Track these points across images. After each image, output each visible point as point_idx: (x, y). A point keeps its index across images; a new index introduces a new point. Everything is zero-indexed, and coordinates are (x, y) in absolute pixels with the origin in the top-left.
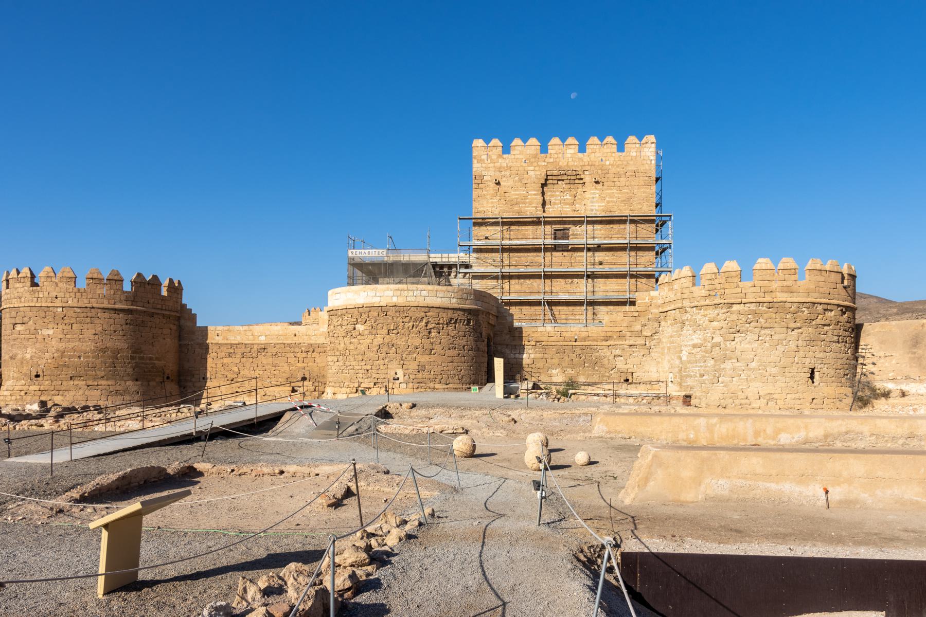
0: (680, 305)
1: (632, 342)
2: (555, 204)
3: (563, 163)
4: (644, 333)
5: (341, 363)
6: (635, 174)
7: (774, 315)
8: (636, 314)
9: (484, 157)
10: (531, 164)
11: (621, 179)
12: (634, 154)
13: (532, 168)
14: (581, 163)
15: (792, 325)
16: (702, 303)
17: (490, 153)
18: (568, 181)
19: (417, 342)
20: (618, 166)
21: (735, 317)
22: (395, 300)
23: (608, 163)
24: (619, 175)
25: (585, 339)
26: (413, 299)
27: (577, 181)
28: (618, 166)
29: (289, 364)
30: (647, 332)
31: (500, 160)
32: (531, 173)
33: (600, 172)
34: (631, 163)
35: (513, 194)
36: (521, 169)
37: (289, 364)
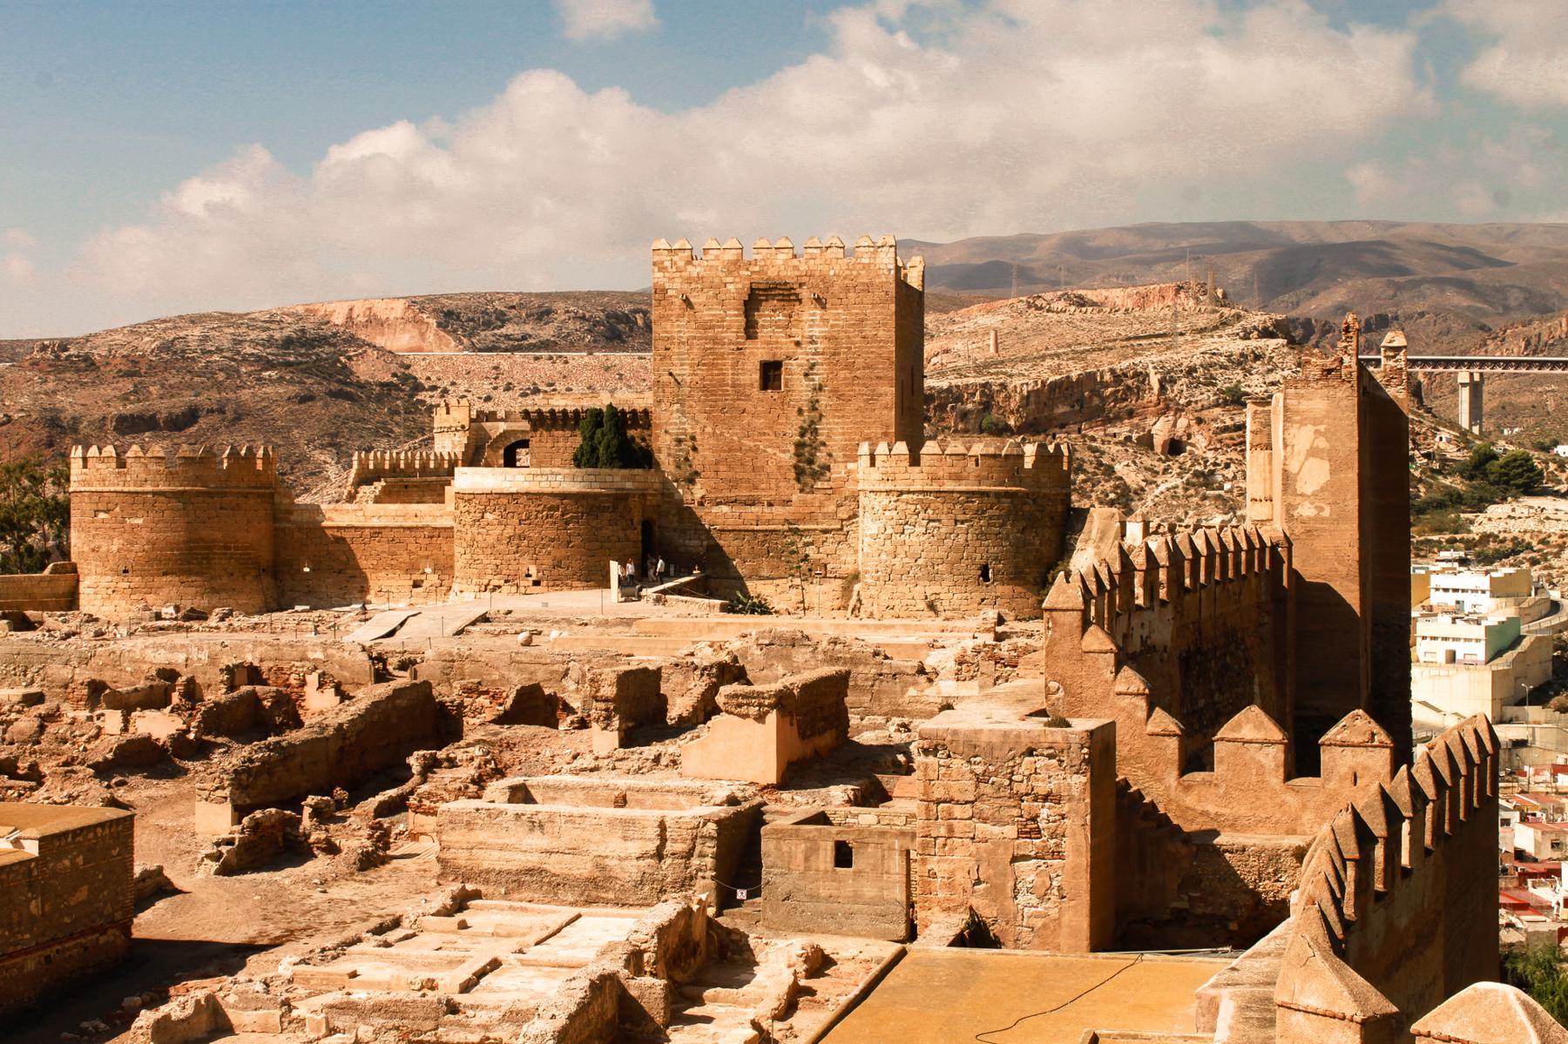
1: (825, 527)
3: (772, 273)
4: (840, 515)
5: (468, 556)
6: (868, 288)
9: (667, 264)
10: (730, 273)
13: (730, 279)
17: (676, 258)
19: (552, 533)
24: (847, 289)
25: (768, 522)
29: (410, 553)
30: (843, 514)
31: (689, 268)
35: (706, 314)
36: (716, 281)
37: (410, 553)
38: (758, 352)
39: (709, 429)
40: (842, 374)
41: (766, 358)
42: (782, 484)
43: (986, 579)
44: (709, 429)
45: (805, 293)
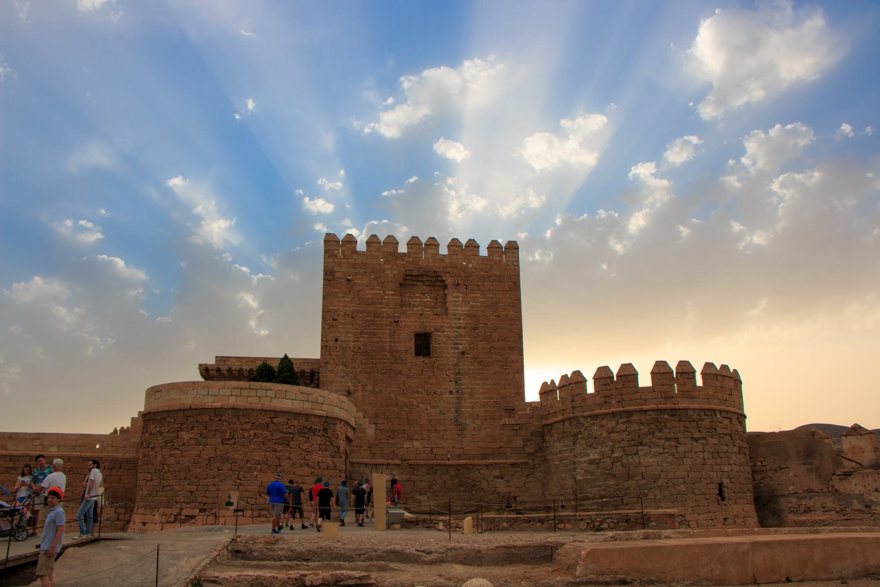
0: (571, 415)
2: (414, 306)
7: (677, 424)
8: (517, 427)
11: (485, 283)
12: (498, 258)
13: (389, 267)
14: (443, 265)
15: (696, 435)
18: (428, 283)
20: (481, 270)
21: (636, 427)
22: (232, 401)
23: (470, 266)
26: (256, 400)
27: (438, 284)
28: (481, 270)
32: (389, 272)
34: (495, 267)
38: (411, 325)
39: (369, 387)
41: (419, 330)
42: (433, 435)
43: (723, 499)
44: (369, 387)
45: (449, 281)
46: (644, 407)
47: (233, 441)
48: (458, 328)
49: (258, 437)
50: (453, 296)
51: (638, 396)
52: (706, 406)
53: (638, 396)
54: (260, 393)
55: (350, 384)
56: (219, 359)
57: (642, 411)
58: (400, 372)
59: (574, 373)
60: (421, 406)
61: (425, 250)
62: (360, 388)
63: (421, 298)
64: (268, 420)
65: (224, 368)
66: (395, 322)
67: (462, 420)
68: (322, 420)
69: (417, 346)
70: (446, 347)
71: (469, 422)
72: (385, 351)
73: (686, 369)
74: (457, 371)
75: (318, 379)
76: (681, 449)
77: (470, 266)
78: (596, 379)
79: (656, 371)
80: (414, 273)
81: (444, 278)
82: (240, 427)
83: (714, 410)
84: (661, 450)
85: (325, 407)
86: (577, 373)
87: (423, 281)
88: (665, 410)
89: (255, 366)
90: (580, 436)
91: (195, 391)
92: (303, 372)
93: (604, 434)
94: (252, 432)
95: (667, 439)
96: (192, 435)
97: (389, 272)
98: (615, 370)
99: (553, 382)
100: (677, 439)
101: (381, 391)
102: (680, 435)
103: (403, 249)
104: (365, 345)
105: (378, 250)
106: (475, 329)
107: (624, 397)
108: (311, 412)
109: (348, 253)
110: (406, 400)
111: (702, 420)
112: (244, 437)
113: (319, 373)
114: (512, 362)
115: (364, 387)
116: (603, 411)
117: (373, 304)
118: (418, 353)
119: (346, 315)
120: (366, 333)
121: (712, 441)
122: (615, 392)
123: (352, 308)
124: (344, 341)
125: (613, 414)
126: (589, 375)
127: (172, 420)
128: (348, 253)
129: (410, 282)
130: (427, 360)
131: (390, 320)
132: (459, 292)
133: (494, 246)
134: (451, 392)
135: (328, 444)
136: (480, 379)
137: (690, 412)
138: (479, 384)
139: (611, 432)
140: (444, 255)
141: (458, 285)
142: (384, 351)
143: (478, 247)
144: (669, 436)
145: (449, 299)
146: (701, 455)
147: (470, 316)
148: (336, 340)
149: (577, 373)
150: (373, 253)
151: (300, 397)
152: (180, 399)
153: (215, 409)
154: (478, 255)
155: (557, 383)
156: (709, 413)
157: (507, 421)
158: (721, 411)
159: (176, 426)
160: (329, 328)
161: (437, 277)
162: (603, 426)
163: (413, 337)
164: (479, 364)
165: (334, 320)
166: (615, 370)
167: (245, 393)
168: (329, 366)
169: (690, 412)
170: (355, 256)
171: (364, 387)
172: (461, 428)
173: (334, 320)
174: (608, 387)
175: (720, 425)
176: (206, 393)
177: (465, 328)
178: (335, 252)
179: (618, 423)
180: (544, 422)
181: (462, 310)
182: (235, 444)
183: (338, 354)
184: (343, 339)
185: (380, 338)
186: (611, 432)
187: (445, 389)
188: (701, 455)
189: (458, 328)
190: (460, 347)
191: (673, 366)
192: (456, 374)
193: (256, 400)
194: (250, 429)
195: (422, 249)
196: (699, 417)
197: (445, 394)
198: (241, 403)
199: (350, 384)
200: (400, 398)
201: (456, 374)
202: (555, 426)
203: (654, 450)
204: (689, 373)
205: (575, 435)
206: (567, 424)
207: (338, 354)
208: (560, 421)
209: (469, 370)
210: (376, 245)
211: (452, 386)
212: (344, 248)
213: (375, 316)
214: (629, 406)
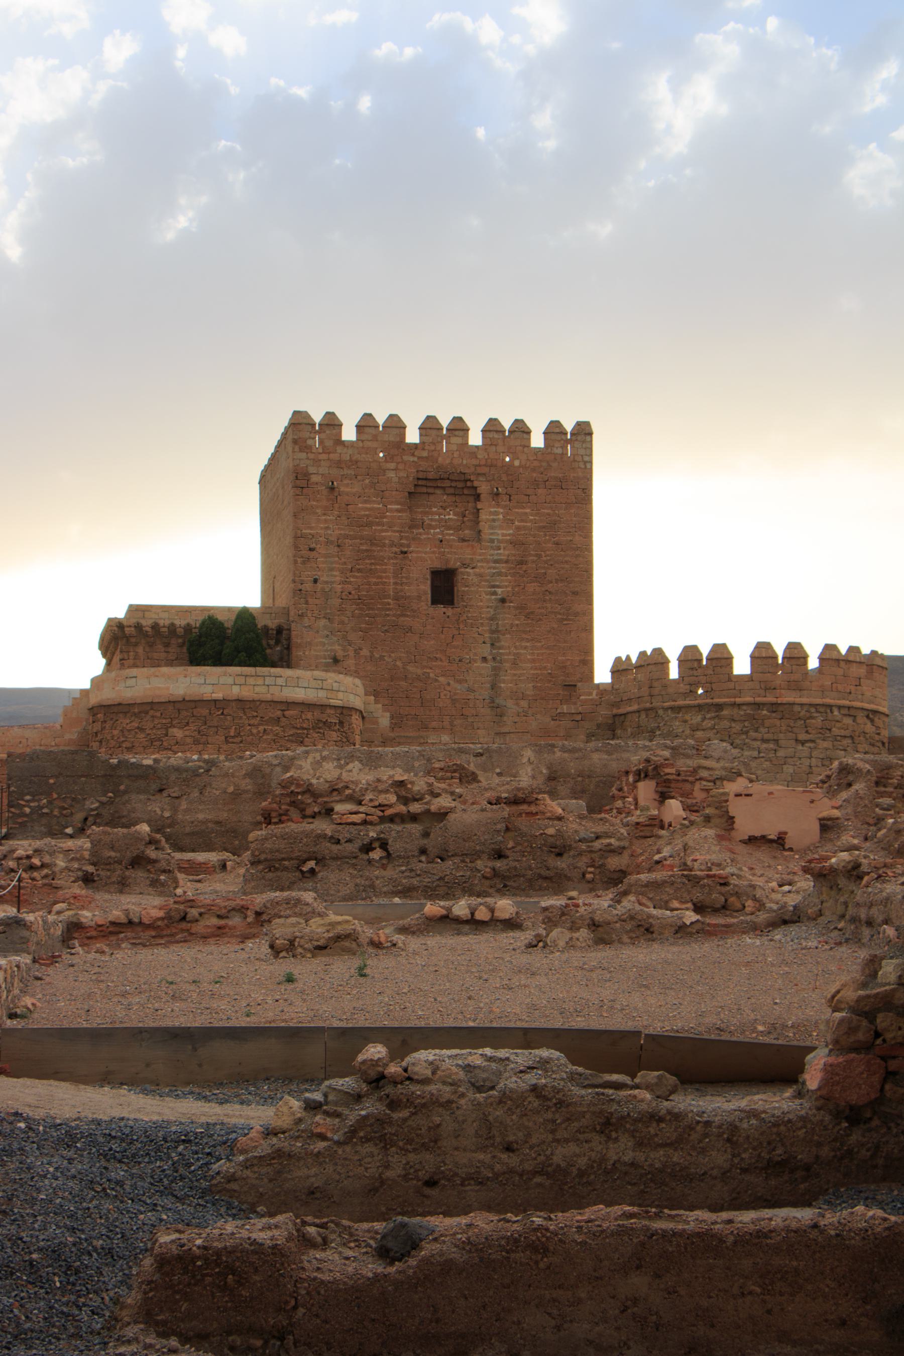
0: (648, 705)
2: (430, 527)
7: (778, 723)
8: (579, 718)
11: (540, 491)
12: (559, 451)
13: (392, 465)
14: (474, 462)
15: (803, 736)
16: (681, 702)
18: (452, 491)
20: (534, 470)
21: (725, 724)
22: (236, 691)
23: (517, 463)
26: (263, 689)
27: (466, 492)
28: (534, 470)
32: (392, 474)
33: (504, 478)
34: (555, 465)
38: (425, 558)
39: (365, 652)
40: (532, 587)
41: (438, 565)
42: (458, 722)
44: (365, 652)
45: (484, 488)
46: (738, 700)
47: (239, 739)
48: (496, 562)
49: (268, 734)
50: (490, 512)
51: (731, 685)
52: (818, 701)
53: (731, 685)
54: (268, 681)
55: (337, 647)
56: (134, 610)
57: (734, 705)
58: (410, 629)
59: (655, 650)
60: (441, 679)
61: (447, 437)
62: (352, 654)
63: (442, 514)
64: (279, 713)
65: (146, 623)
66: (402, 552)
67: (499, 701)
68: (338, 711)
69: (434, 589)
70: (478, 591)
71: (510, 703)
72: (388, 597)
73: (796, 654)
74: (494, 627)
75: (289, 639)
76: (781, 753)
77: (517, 463)
78: (682, 661)
79: (756, 655)
80: (431, 475)
81: (476, 484)
82: (247, 722)
83: (830, 707)
84: (755, 754)
85: (341, 695)
86: (658, 652)
87: (444, 488)
88: (764, 704)
89: (195, 621)
90: (658, 733)
91: (188, 679)
92: (266, 629)
93: (688, 732)
94: (261, 728)
95: (764, 741)
96: (187, 733)
97: (392, 474)
98: (705, 651)
99: (628, 658)
100: (776, 741)
101: (382, 658)
102: (781, 736)
103: (412, 436)
104: (358, 589)
105: (375, 438)
106: (521, 563)
107: (714, 686)
108: (325, 702)
109: (329, 443)
110: (419, 671)
111: (811, 718)
112: (252, 734)
113: (289, 630)
114: (576, 614)
115: (357, 651)
116: (687, 702)
117: (369, 524)
118: (435, 602)
119: (328, 542)
120: (359, 570)
121: (826, 744)
122: (703, 679)
123: (337, 532)
124: (327, 582)
125: (700, 707)
126: (673, 655)
127: (158, 714)
128: (329, 443)
129: (424, 490)
130: (449, 611)
131: (394, 549)
132: (498, 505)
133: (554, 430)
134: (484, 659)
135: (345, 740)
136: (528, 640)
137: (797, 708)
138: (526, 648)
139: (695, 729)
140: (477, 447)
141: (497, 494)
142: (388, 597)
143: (528, 432)
144: (766, 736)
145: (483, 516)
146: (807, 762)
147: (514, 543)
148: (315, 581)
149: (658, 652)
150: (369, 444)
151: (314, 684)
152: (168, 689)
153: (215, 701)
154: (529, 446)
155: (634, 660)
156: (822, 710)
157: (565, 708)
158: (840, 707)
159: (164, 721)
160: (304, 563)
161: (466, 481)
162: (686, 721)
163: (429, 577)
164: (527, 617)
165: (311, 550)
166: (705, 651)
167: (251, 681)
168: (306, 620)
169: (797, 708)
170: (339, 449)
171: (357, 651)
172: (499, 712)
173: (311, 550)
174: (695, 673)
175: (838, 725)
176: (203, 681)
177: (507, 562)
178: (310, 442)
179: (704, 719)
180: (615, 711)
181: (502, 533)
182: (241, 742)
183: (317, 602)
184: (324, 579)
185: (381, 577)
186: (695, 729)
187: (475, 654)
188: (807, 762)
189: (496, 562)
190: (499, 591)
191: (780, 651)
192: (492, 632)
193: (263, 689)
194: (259, 725)
195: (443, 437)
196: (808, 715)
197: (475, 661)
198: (246, 693)
199: (337, 647)
200: (411, 668)
201: (492, 632)
202: (629, 717)
203: (746, 753)
204: (799, 658)
205: (653, 731)
206: (643, 716)
207: (317, 602)
208: (634, 712)
209: (512, 625)
210: (372, 431)
211: (486, 650)
212: (323, 436)
213: (372, 544)
214: (719, 697)
